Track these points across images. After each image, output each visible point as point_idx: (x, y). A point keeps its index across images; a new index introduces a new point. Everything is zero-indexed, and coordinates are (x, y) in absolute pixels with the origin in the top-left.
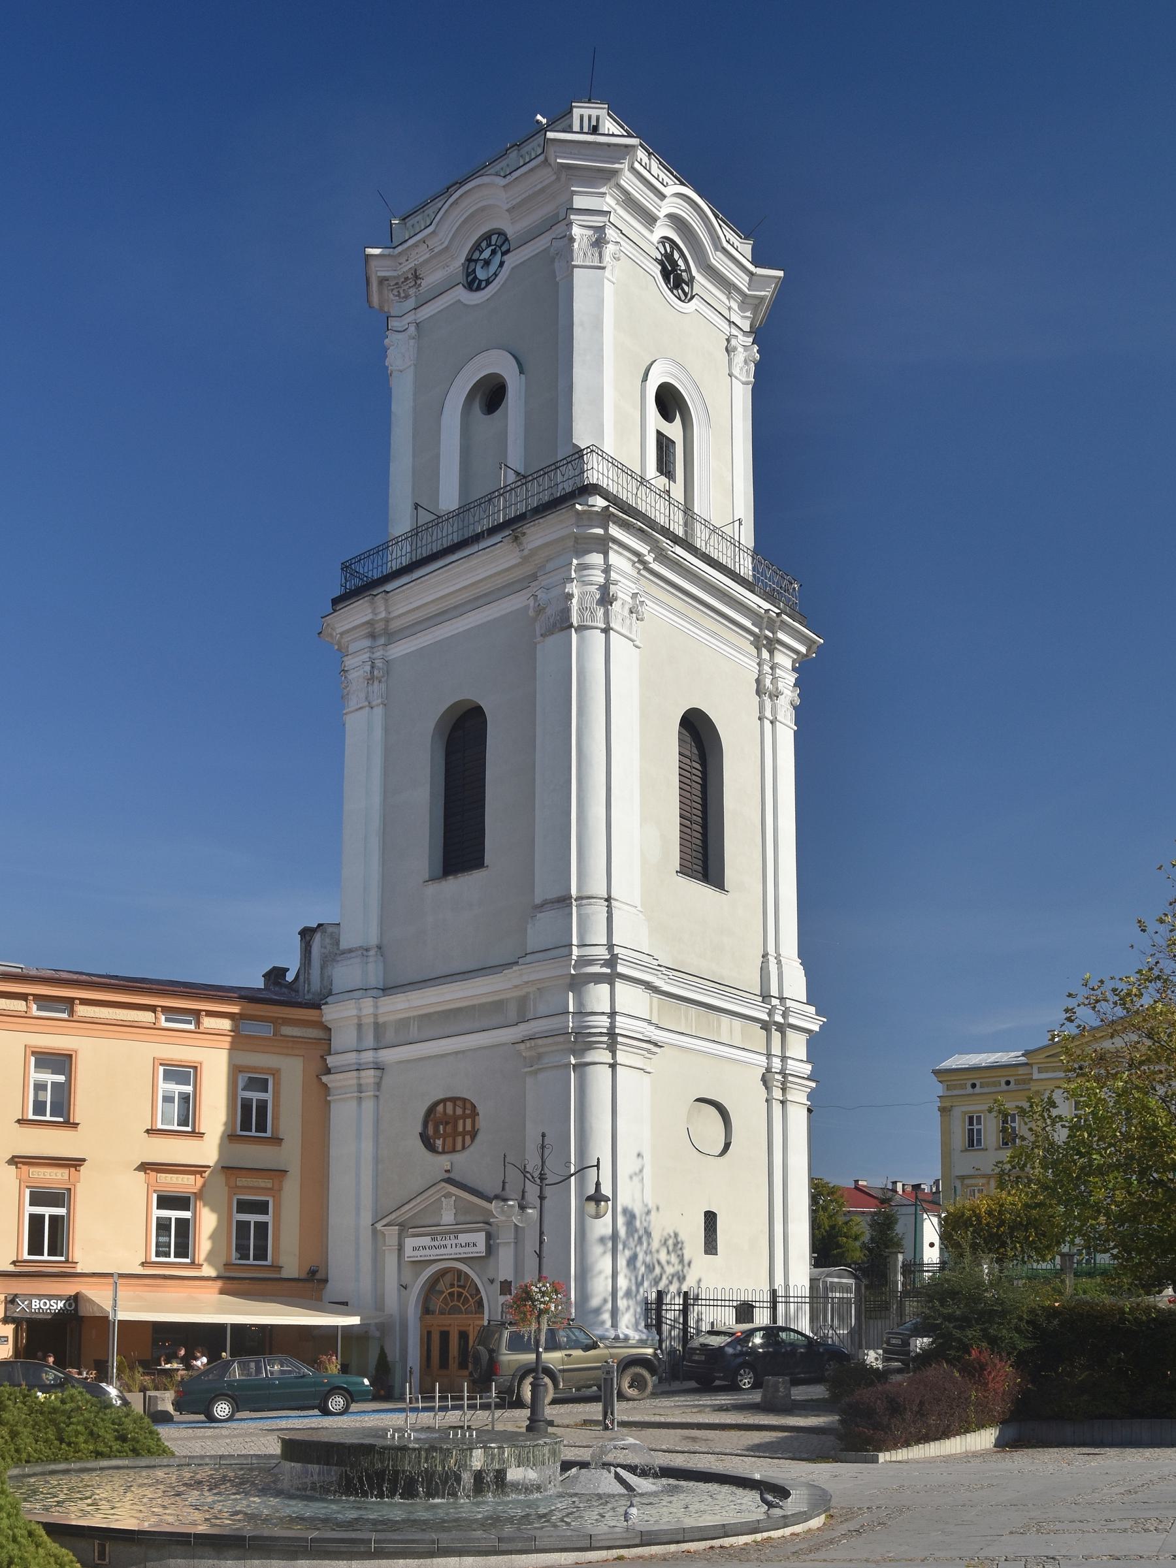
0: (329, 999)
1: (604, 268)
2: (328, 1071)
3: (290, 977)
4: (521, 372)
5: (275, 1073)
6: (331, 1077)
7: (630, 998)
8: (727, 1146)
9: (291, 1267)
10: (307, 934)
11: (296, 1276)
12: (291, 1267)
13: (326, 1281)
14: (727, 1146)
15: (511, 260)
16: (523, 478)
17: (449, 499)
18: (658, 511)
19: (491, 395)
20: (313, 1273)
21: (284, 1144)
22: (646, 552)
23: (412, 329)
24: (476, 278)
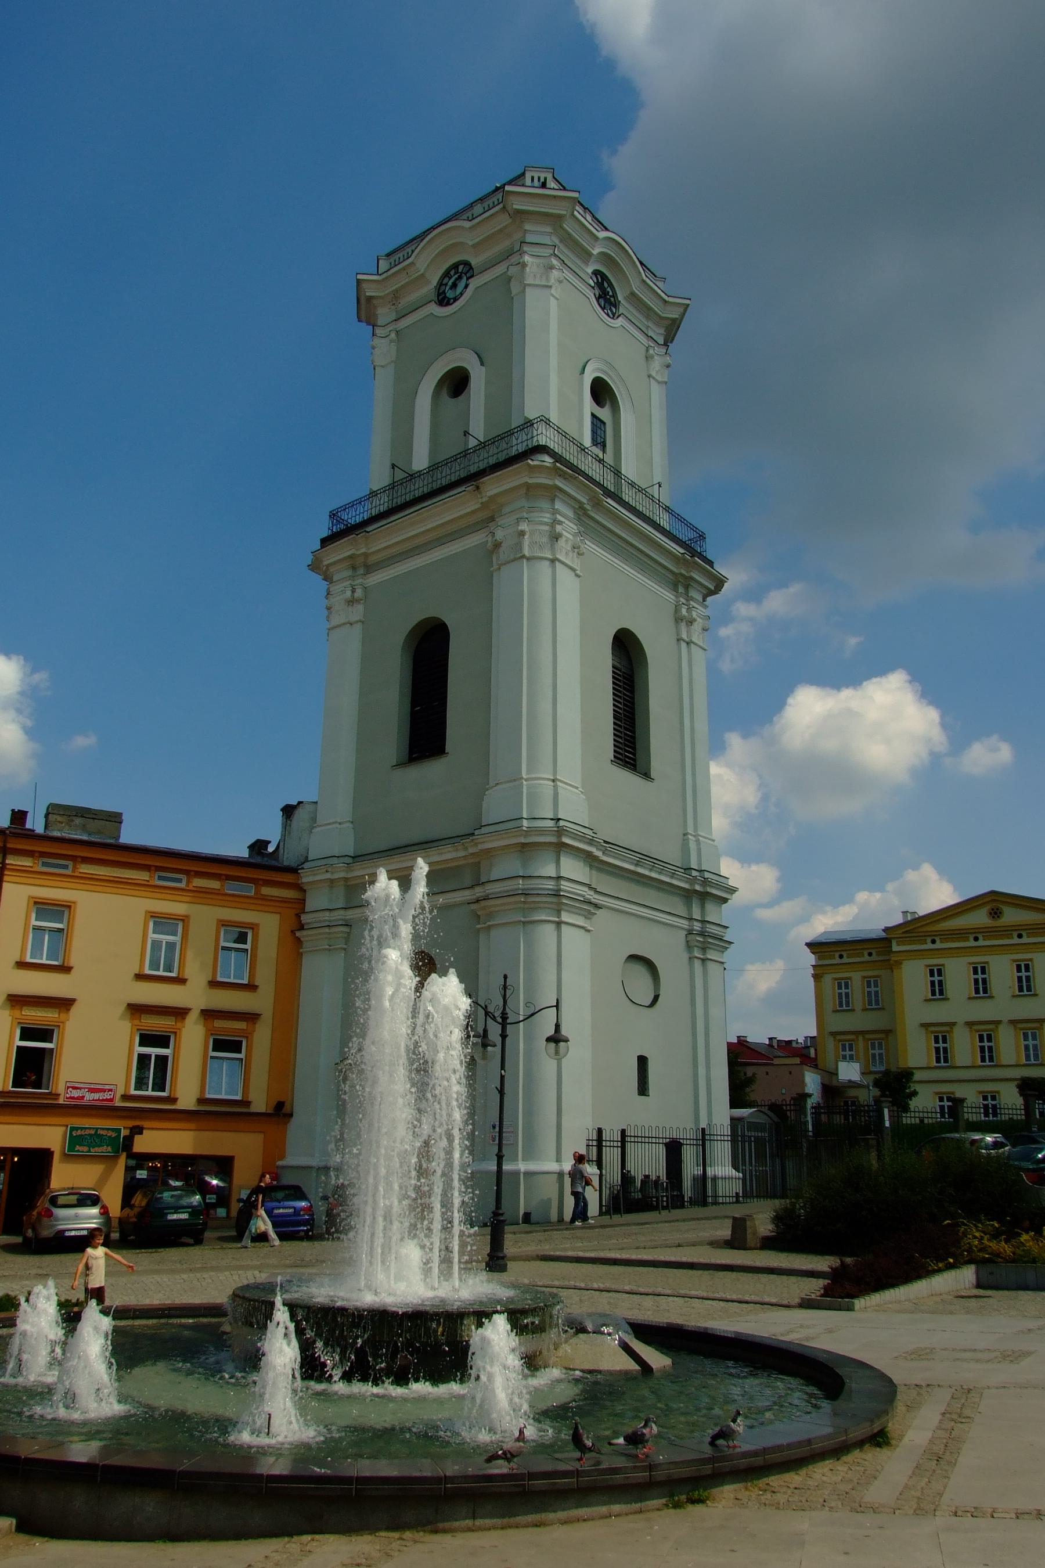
0: (306, 866)
1: (551, 287)
2: (302, 927)
3: (271, 849)
4: (482, 364)
5: (254, 927)
6: (305, 933)
7: (571, 868)
8: (656, 998)
9: (260, 1104)
10: (288, 811)
11: (264, 1111)
12: (260, 1104)
13: (291, 1115)
14: (656, 998)
15: (474, 283)
16: (482, 445)
17: (420, 461)
18: (594, 470)
19: (457, 383)
20: (280, 1105)
21: (259, 990)
22: (585, 501)
23: (393, 335)
24: (445, 297)
